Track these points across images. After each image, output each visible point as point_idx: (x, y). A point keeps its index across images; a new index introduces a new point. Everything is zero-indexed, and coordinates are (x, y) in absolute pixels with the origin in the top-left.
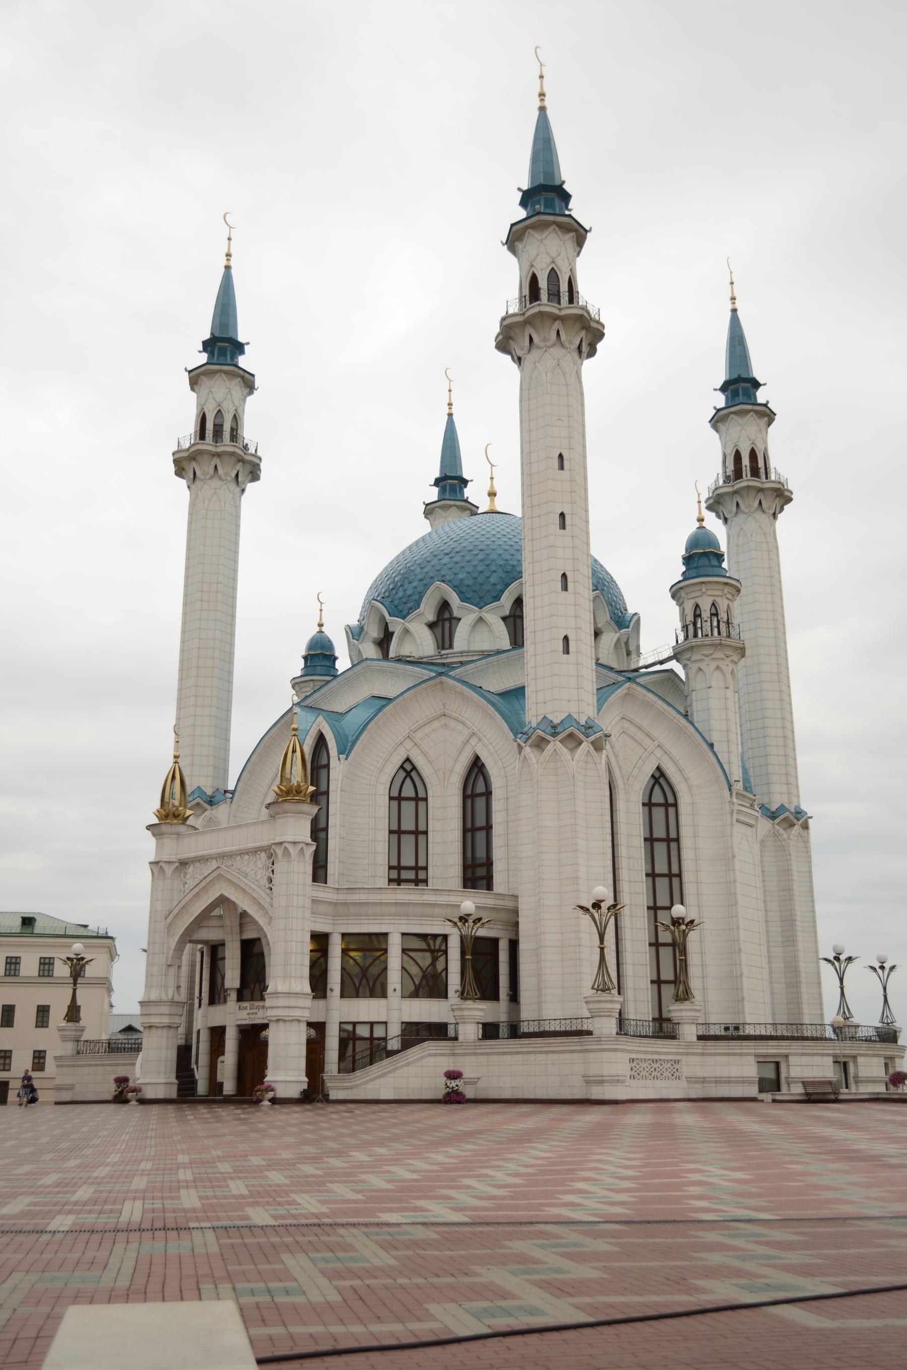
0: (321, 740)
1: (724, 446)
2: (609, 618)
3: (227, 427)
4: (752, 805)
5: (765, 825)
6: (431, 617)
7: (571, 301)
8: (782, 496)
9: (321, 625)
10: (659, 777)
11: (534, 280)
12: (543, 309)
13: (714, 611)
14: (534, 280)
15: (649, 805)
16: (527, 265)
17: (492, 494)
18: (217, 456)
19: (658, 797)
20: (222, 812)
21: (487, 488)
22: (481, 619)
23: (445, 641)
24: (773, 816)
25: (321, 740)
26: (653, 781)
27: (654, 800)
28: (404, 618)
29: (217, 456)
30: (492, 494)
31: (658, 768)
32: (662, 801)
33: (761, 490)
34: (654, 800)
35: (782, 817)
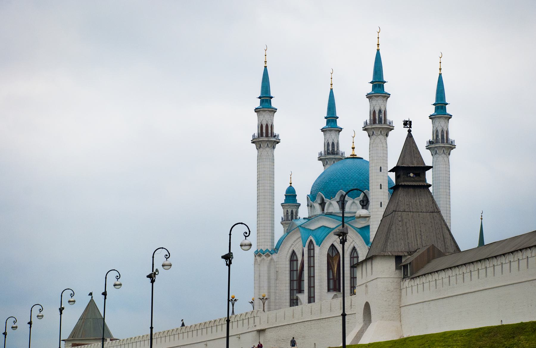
0: (311, 241)
1: (433, 127)
6: (338, 200)
7: (385, 123)
8: (452, 146)
9: (291, 183)
11: (374, 112)
12: (377, 126)
14: (374, 112)
16: (372, 108)
17: (353, 148)
18: (266, 138)
20: (275, 256)
21: (352, 146)
22: (354, 202)
23: (343, 207)
25: (311, 241)
28: (330, 199)
29: (266, 138)
30: (353, 148)
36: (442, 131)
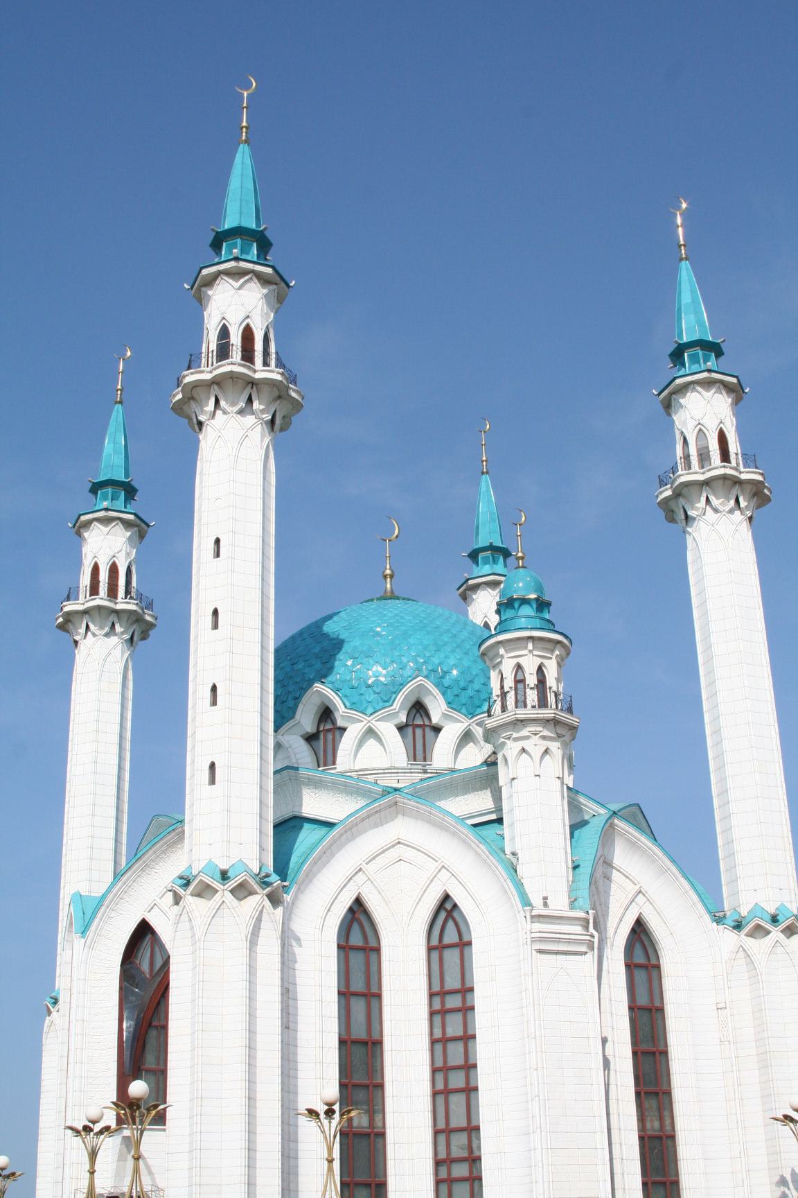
2: (444, 706)
3: (104, 576)
4: (587, 928)
5: (730, 938)
10: (446, 908)
13: (520, 677)
15: (436, 948)
19: (451, 936)
24: (738, 926)
26: (443, 915)
27: (446, 941)
31: (447, 897)
32: (456, 939)
33: (707, 483)
34: (446, 941)
35: (751, 925)
36: (701, 433)
